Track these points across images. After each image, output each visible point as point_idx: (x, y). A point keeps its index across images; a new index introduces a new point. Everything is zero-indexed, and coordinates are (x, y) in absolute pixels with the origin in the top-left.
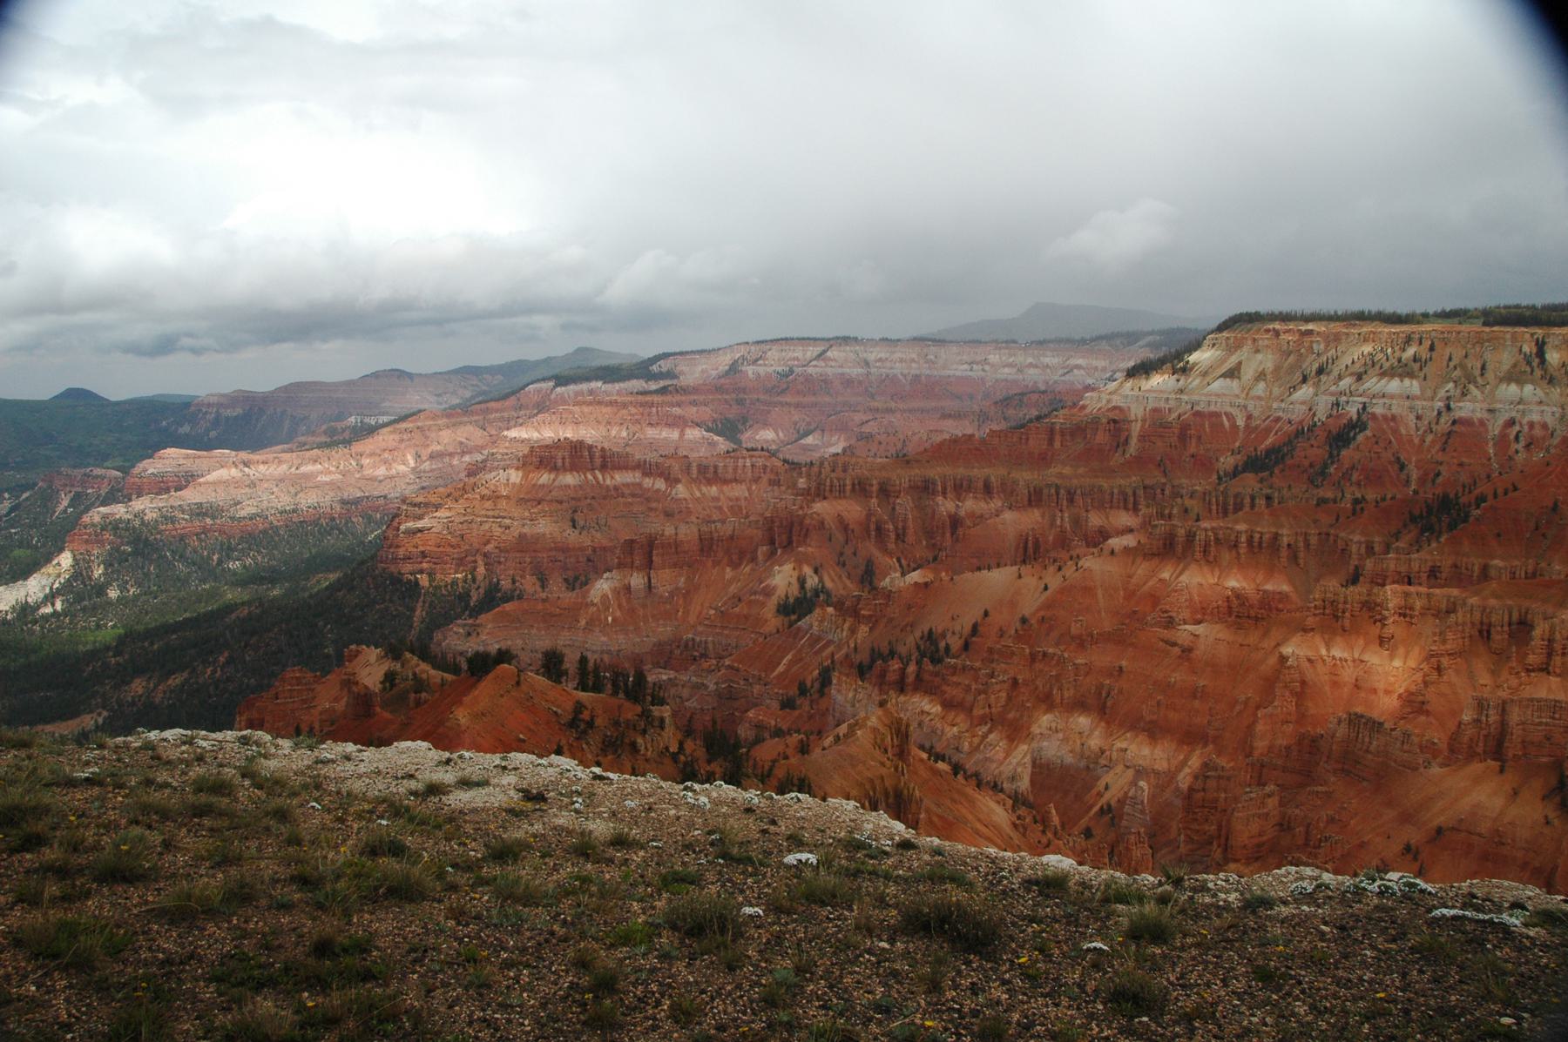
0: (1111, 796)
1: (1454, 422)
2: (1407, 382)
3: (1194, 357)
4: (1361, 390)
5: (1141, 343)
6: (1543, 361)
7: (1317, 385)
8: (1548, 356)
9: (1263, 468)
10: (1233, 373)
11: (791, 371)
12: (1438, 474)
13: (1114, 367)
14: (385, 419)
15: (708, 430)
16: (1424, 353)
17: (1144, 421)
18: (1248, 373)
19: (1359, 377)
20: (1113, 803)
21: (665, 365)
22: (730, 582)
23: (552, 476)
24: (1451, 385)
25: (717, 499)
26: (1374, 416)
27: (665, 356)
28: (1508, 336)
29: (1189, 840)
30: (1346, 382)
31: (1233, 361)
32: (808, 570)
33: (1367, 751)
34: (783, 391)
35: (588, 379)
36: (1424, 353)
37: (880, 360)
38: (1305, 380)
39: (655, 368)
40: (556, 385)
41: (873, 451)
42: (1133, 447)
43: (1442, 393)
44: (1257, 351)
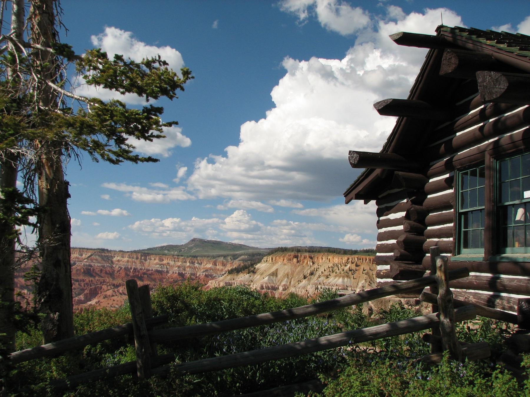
3: (258, 266)
4: (327, 282)
5: (239, 259)
13: (226, 269)
16: (353, 267)
18: (280, 275)
24: (363, 281)
31: (273, 269)
36: (353, 267)
37: (119, 261)
38: (305, 277)
41: (111, 304)
43: (360, 285)
44: (285, 264)
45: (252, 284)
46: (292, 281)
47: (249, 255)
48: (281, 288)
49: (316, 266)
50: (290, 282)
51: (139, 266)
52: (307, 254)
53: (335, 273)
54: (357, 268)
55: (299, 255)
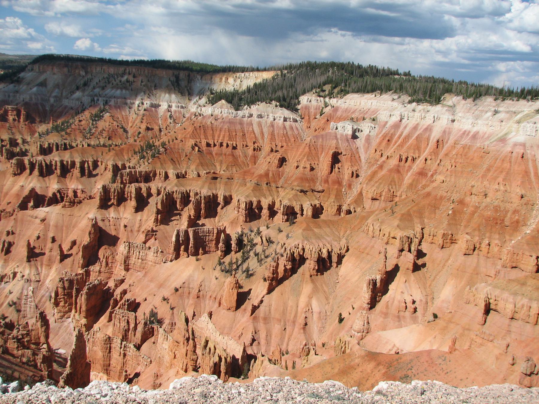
0: (13, 297)
1: (145, 110)
2: (124, 91)
3: (22, 75)
4: (104, 94)
6: (178, 85)
7: (83, 91)
8: (180, 82)
12: (139, 133)
16: (131, 78)
18: (50, 84)
19: (103, 88)
20: (15, 300)
28: (164, 73)
29: (60, 312)
30: (97, 90)
31: (42, 78)
33: (139, 259)
38: (78, 88)
44: (54, 74)
45: (18, 95)
46: (64, 92)
48: (52, 100)
49: (89, 76)
50: (62, 94)
52: (79, 64)
53: (111, 84)
54: (135, 80)
55: (70, 64)
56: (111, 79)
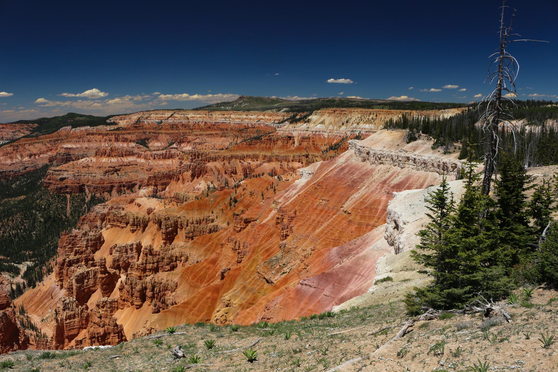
3: (310, 117)
9: (335, 149)
10: (323, 123)
11: (162, 122)
13: (274, 119)
14: (6, 142)
15: (137, 143)
17: (298, 137)
18: (327, 122)
21: (112, 120)
22: (183, 188)
23: (107, 159)
25: (162, 165)
26: (362, 134)
27: (112, 116)
30: (355, 125)
32: (209, 183)
34: (160, 129)
35: (85, 125)
36: (375, 117)
37: (192, 117)
39: (108, 121)
40: (72, 128)
42: (297, 144)
47: (290, 107)
51: (208, 120)
56: (363, 118)
